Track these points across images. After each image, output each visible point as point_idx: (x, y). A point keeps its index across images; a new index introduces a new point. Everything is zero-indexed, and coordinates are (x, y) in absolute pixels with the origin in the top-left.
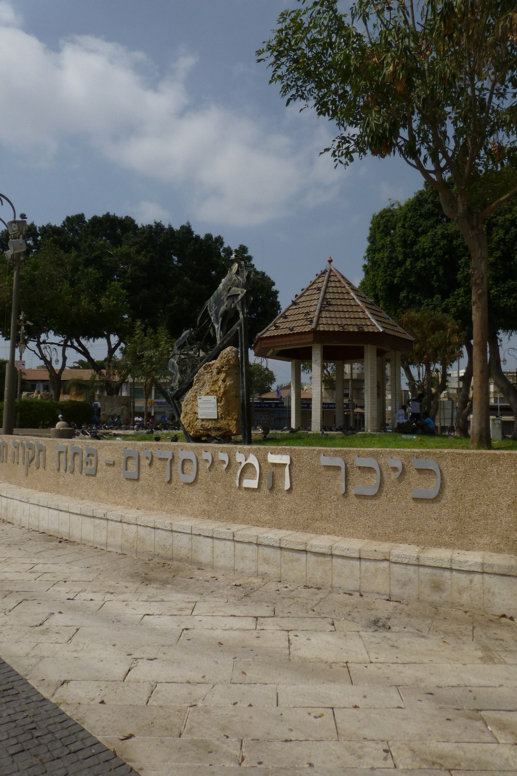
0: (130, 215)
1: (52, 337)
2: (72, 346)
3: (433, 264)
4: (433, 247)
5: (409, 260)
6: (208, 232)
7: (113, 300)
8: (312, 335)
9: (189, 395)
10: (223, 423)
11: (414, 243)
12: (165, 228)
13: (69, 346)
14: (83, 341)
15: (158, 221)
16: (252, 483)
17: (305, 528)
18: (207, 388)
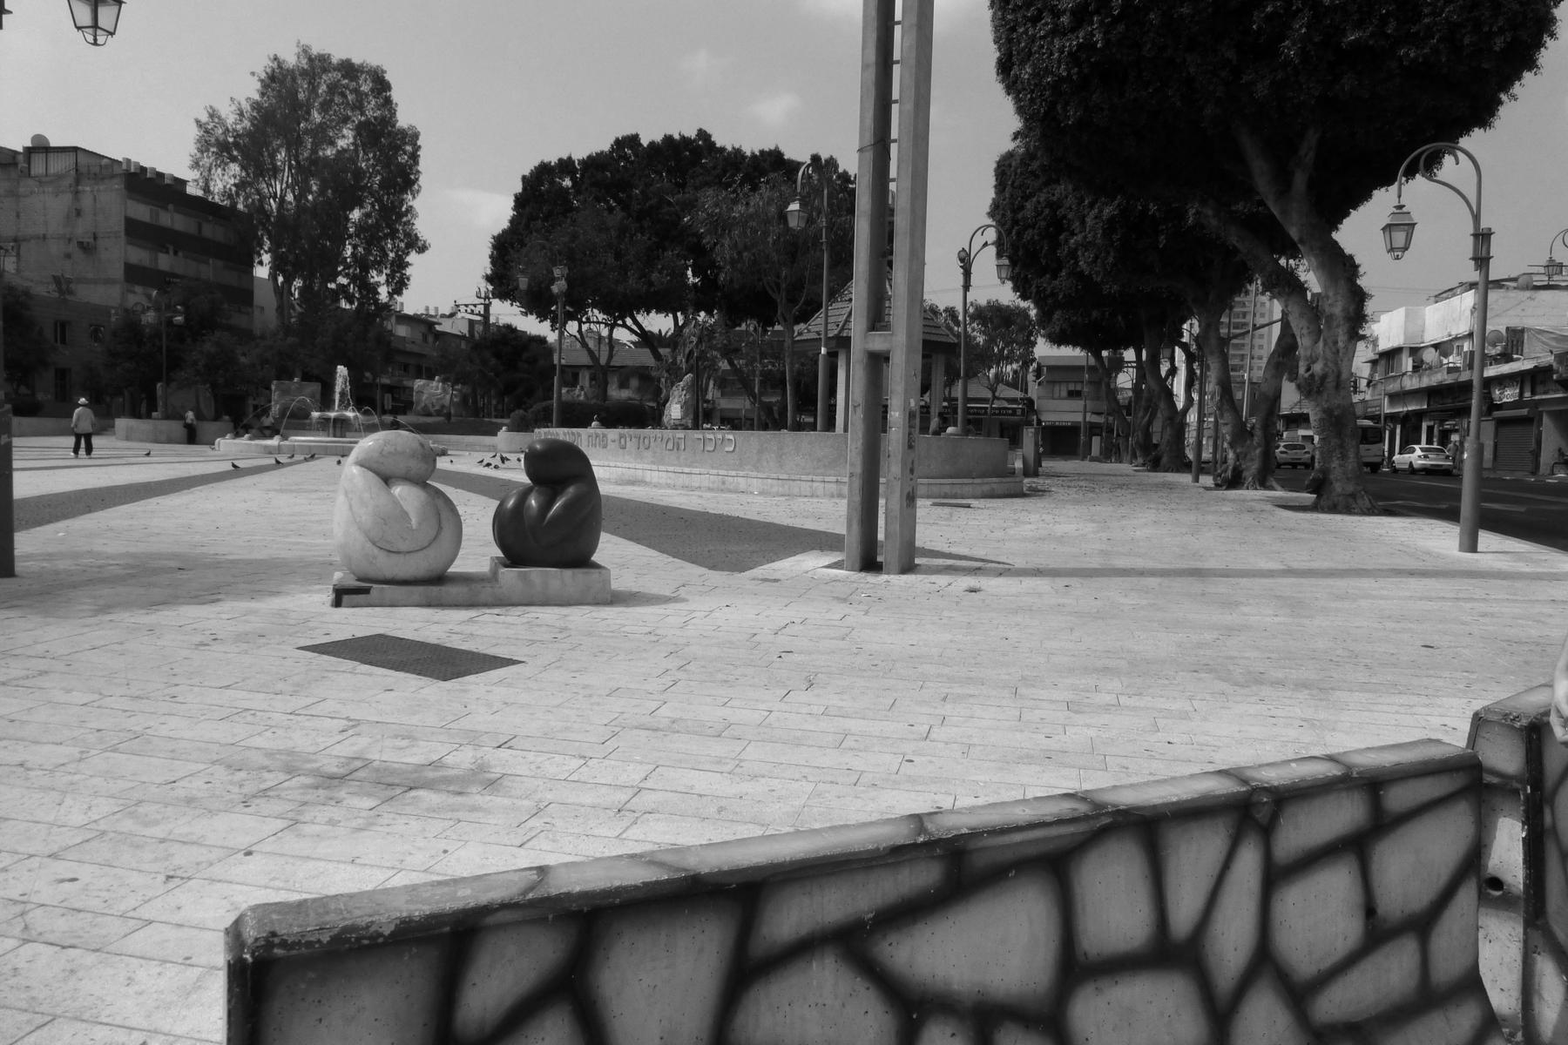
0: (704, 128)
1: (597, 314)
2: (625, 325)
3: (1036, 238)
4: (1035, 217)
5: (1016, 228)
6: (815, 152)
7: (667, 275)
8: (834, 342)
9: (668, 405)
10: (684, 422)
11: (1022, 208)
12: (747, 157)
13: (619, 325)
14: (639, 318)
15: (737, 146)
16: (670, 446)
17: (689, 466)
18: (676, 400)
